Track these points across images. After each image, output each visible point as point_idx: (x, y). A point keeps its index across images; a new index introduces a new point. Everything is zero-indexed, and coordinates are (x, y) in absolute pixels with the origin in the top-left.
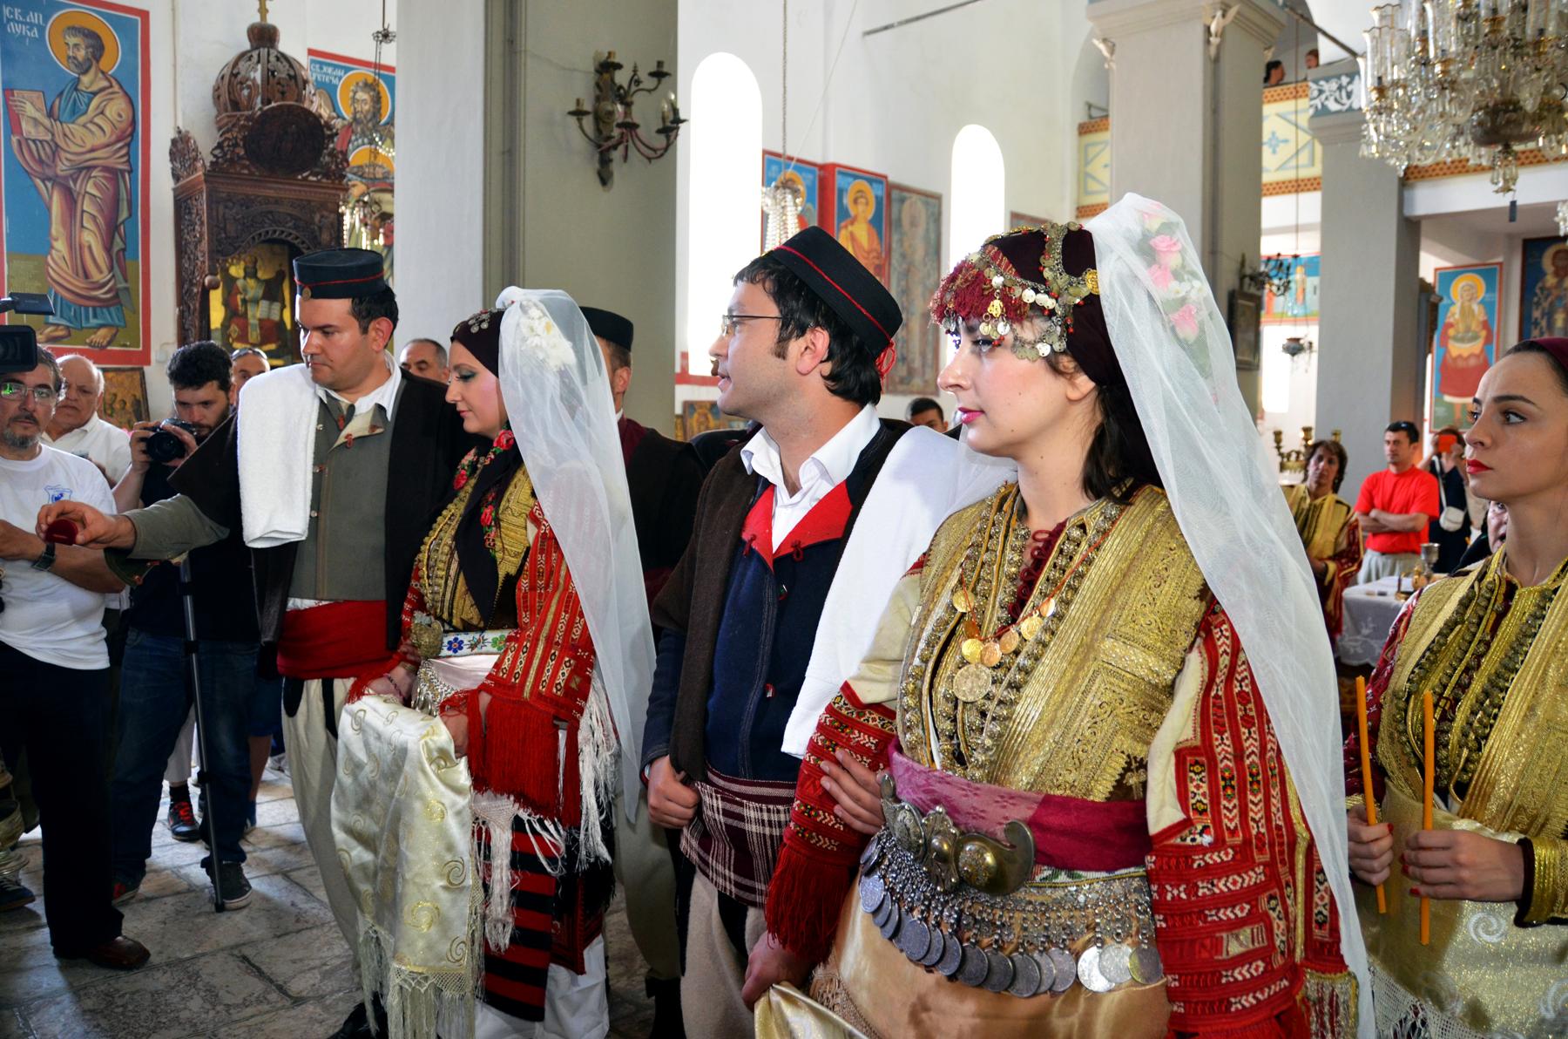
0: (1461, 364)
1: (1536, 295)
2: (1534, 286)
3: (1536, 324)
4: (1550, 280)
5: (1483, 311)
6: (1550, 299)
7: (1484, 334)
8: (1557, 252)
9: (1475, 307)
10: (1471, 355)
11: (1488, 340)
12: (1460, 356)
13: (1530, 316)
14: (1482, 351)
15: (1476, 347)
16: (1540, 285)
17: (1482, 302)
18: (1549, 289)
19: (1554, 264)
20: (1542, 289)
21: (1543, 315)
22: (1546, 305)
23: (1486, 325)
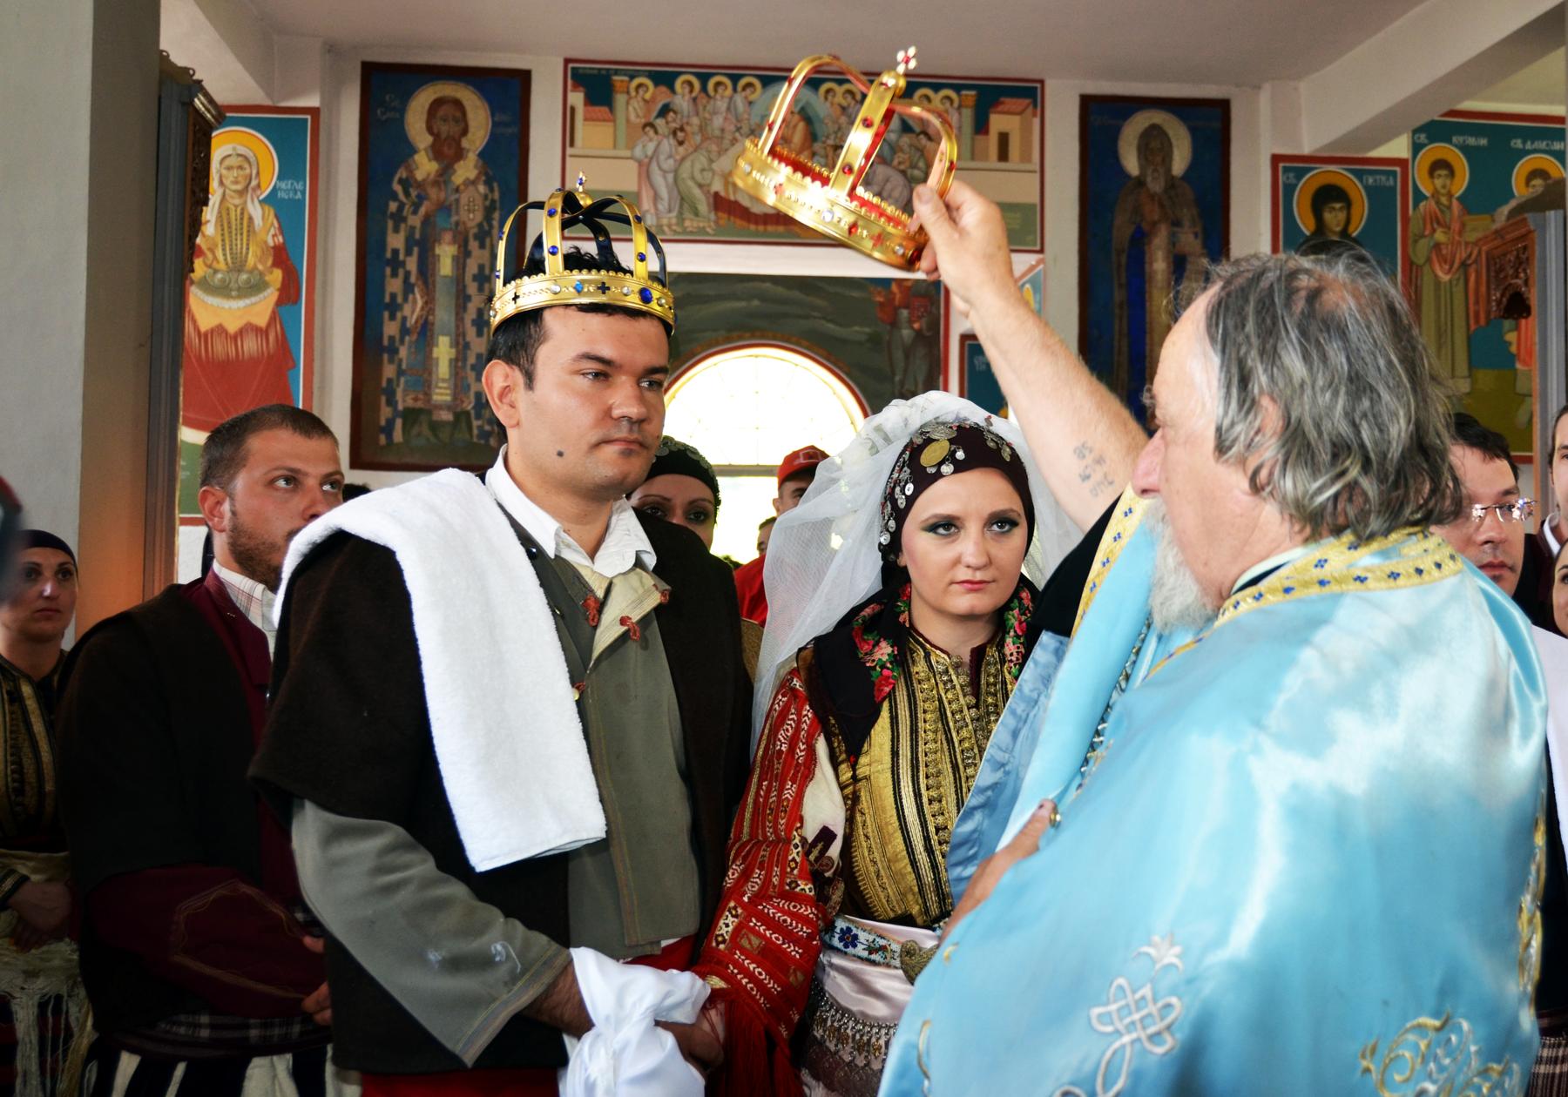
0: (220, 348)
1: (394, 197)
2: (390, 182)
3: (396, 264)
4: (425, 166)
5: (272, 218)
6: (423, 210)
7: (277, 276)
8: (437, 104)
9: (256, 210)
10: (249, 328)
11: (289, 294)
12: (220, 330)
13: (382, 244)
14: (274, 317)
15: (259, 309)
16: (402, 173)
17: (271, 200)
18: (420, 185)
19: (430, 129)
20: (406, 184)
21: (410, 243)
22: (415, 221)
23: (281, 257)
